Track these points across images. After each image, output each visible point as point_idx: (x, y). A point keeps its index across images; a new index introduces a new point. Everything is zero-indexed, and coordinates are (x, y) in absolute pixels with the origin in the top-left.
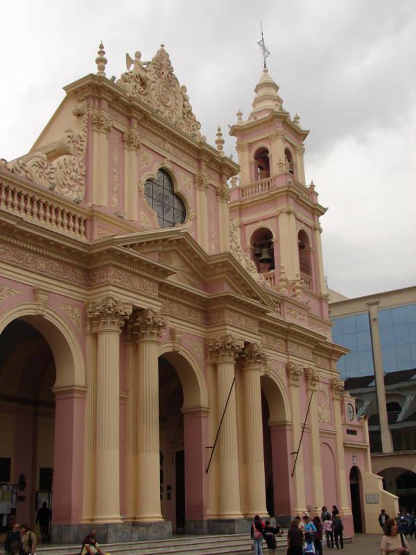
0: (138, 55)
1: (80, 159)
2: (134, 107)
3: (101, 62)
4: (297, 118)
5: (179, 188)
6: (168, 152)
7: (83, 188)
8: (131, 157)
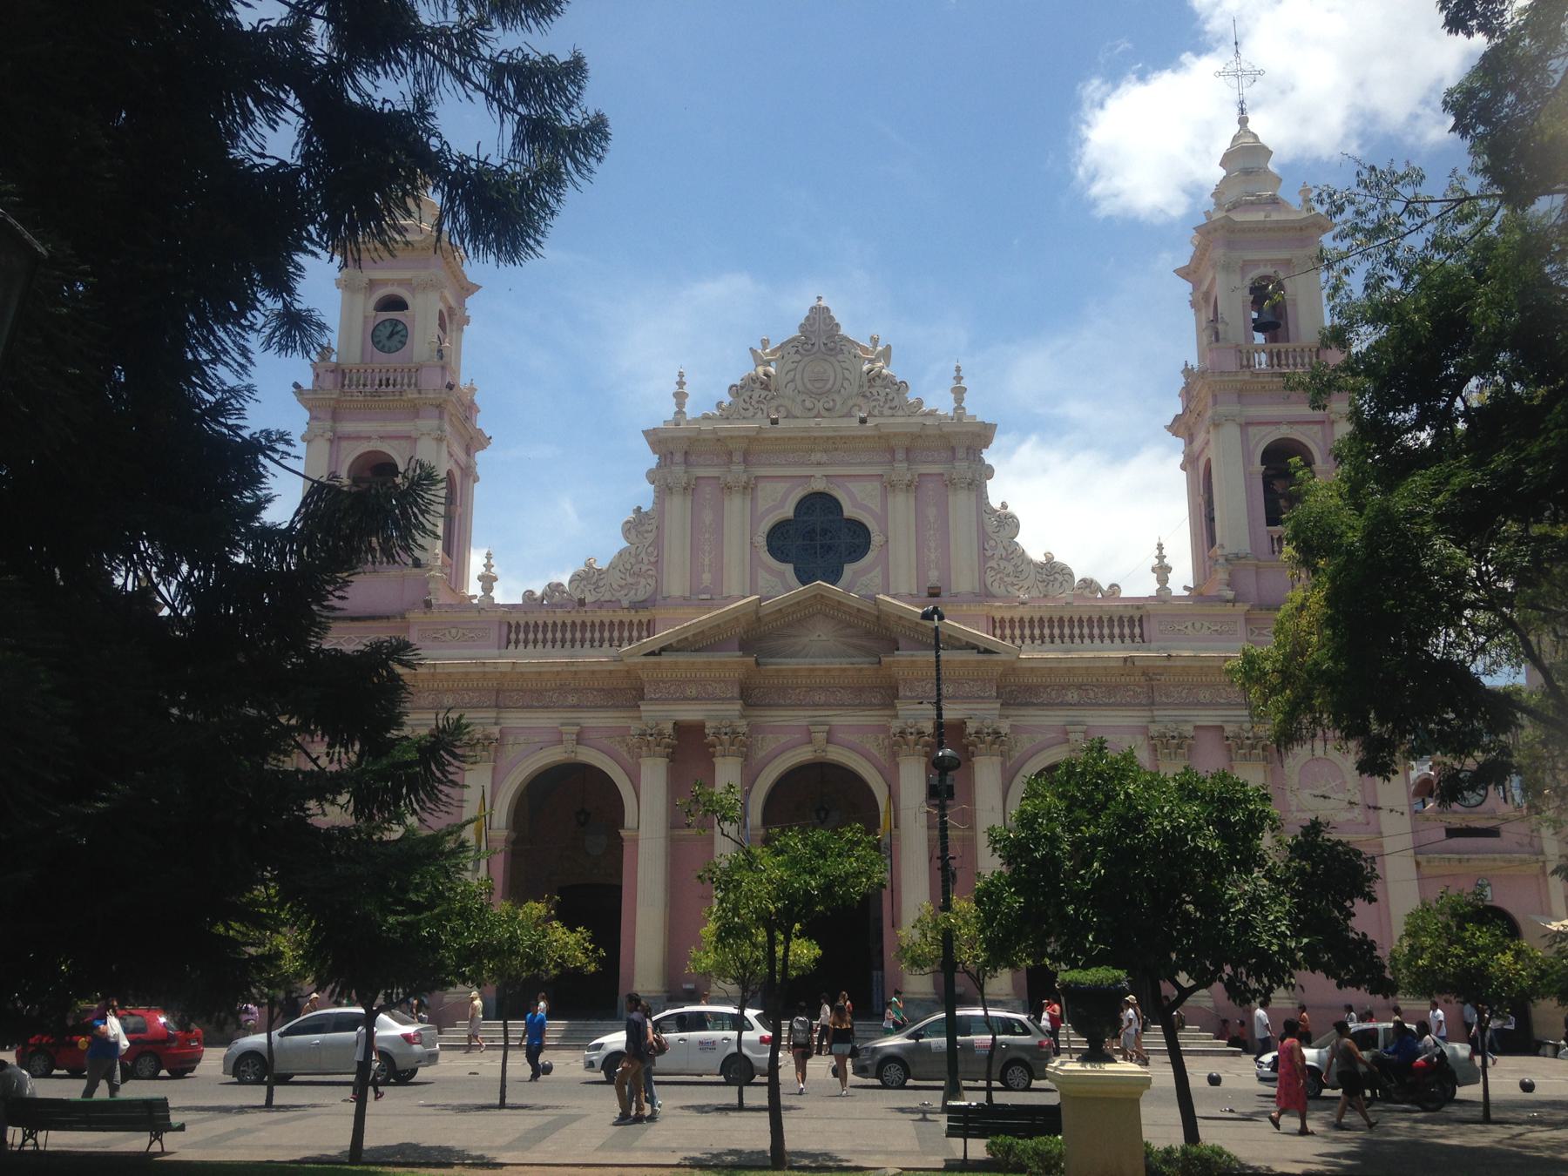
0: (765, 343)
2: (725, 438)
3: (680, 397)
5: (849, 511)
6: (819, 464)
7: (653, 583)
8: (735, 507)
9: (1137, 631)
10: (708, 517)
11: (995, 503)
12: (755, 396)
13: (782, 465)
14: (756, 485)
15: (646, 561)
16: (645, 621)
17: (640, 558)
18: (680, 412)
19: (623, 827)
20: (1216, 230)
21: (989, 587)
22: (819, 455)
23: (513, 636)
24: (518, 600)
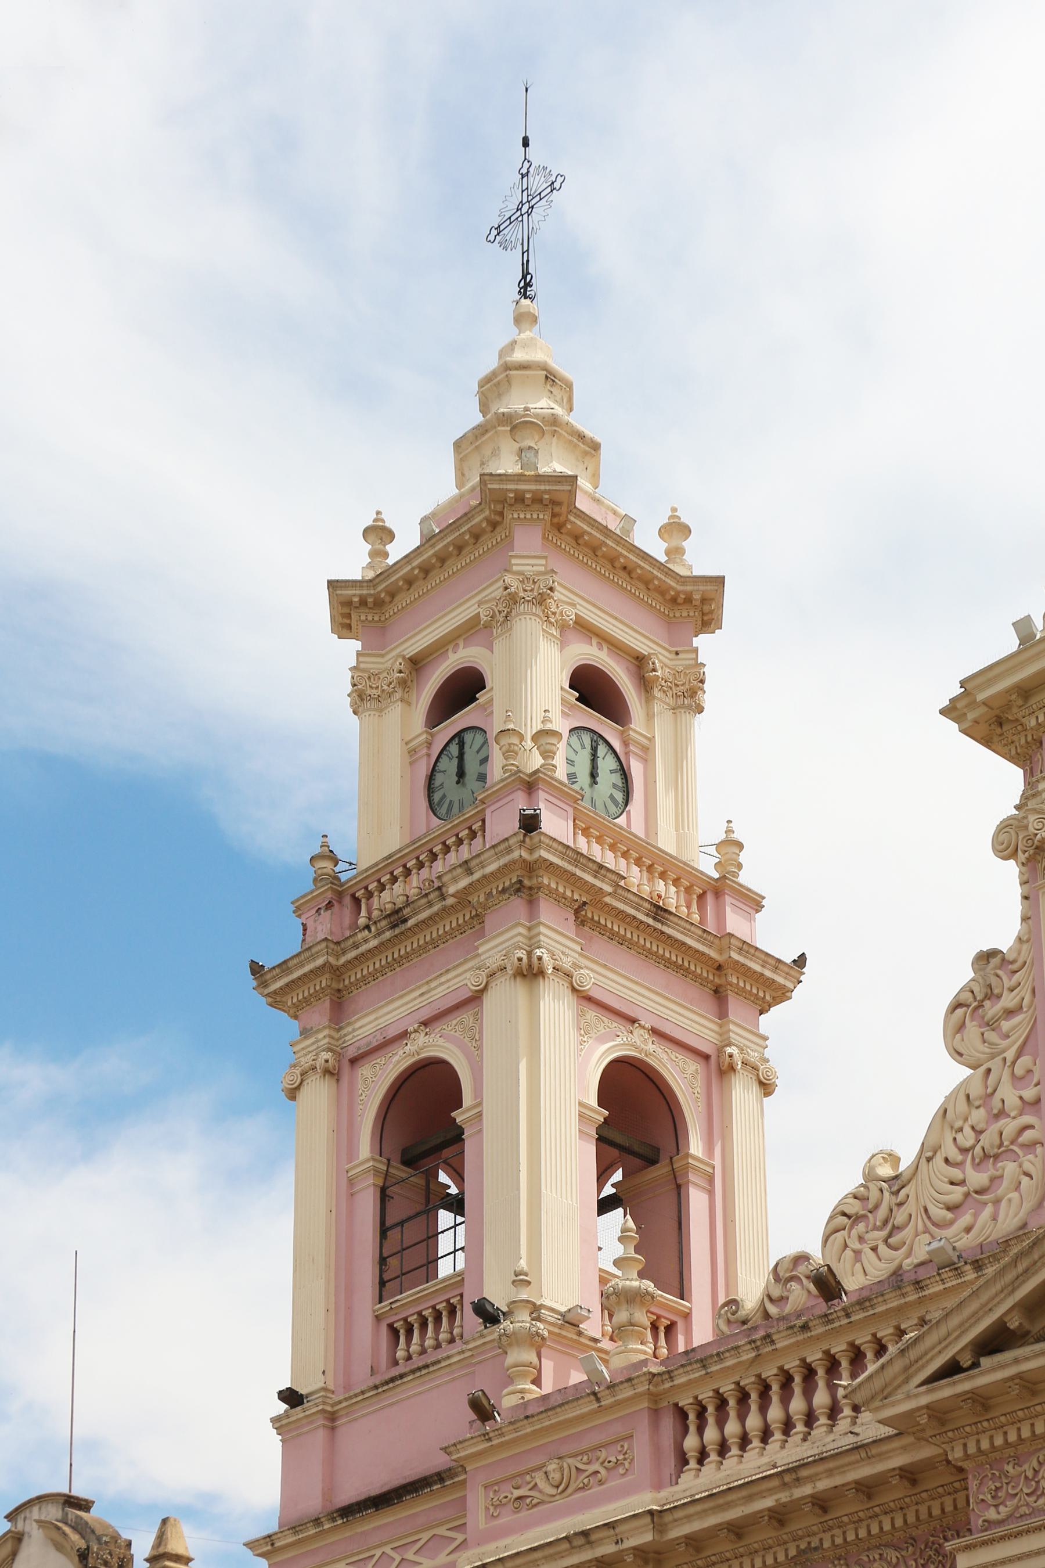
1: (1010, 1055)
17: (996, 1104)
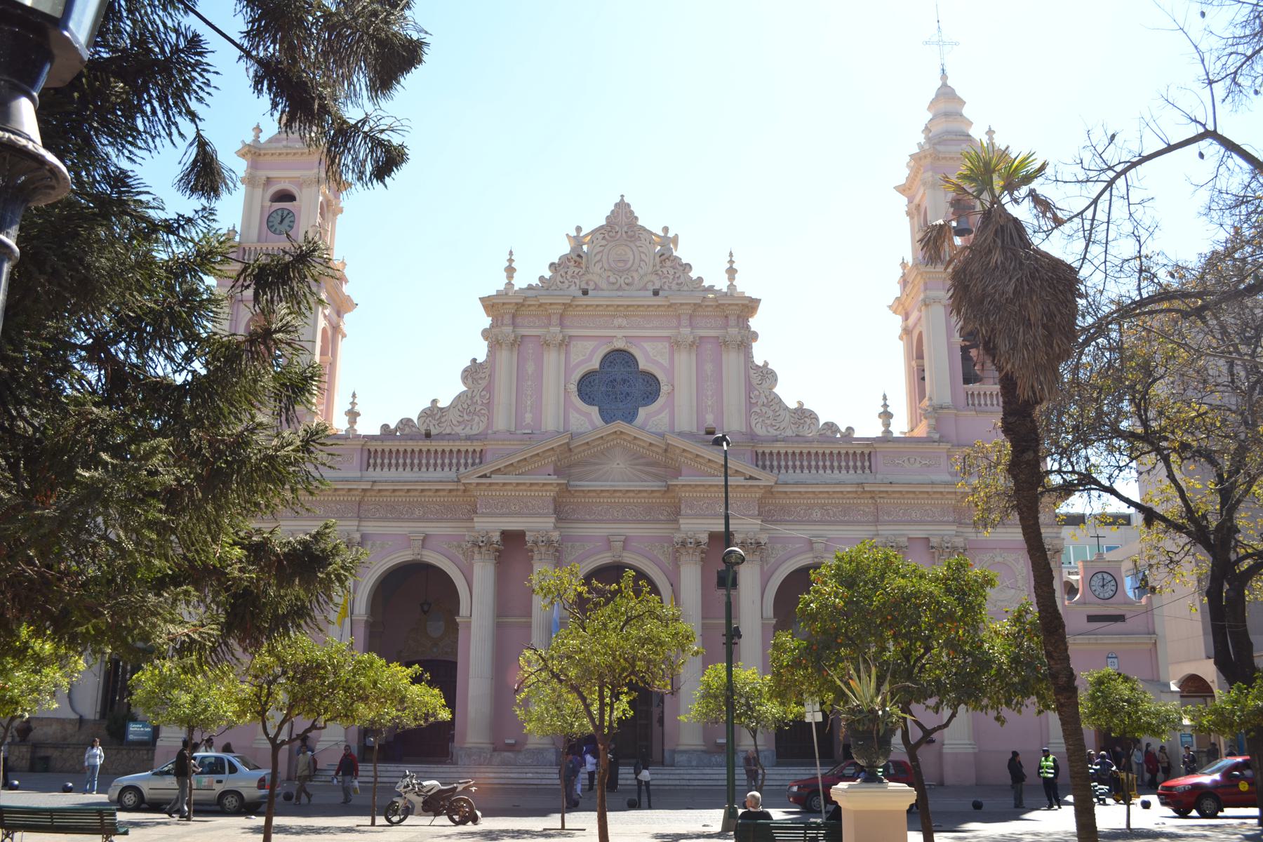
0: (579, 229)
3: (510, 270)
4: (990, 132)
5: (643, 365)
6: (620, 327)
8: (552, 359)
9: (867, 464)
10: (530, 368)
11: (759, 361)
12: (570, 273)
13: (591, 328)
14: (569, 343)
15: (479, 402)
16: (478, 449)
18: (510, 284)
19: (458, 615)
20: (925, 157)
21: (753, 426)
22: (620, 320)
23: (372, 461)
24: (376, 431)
